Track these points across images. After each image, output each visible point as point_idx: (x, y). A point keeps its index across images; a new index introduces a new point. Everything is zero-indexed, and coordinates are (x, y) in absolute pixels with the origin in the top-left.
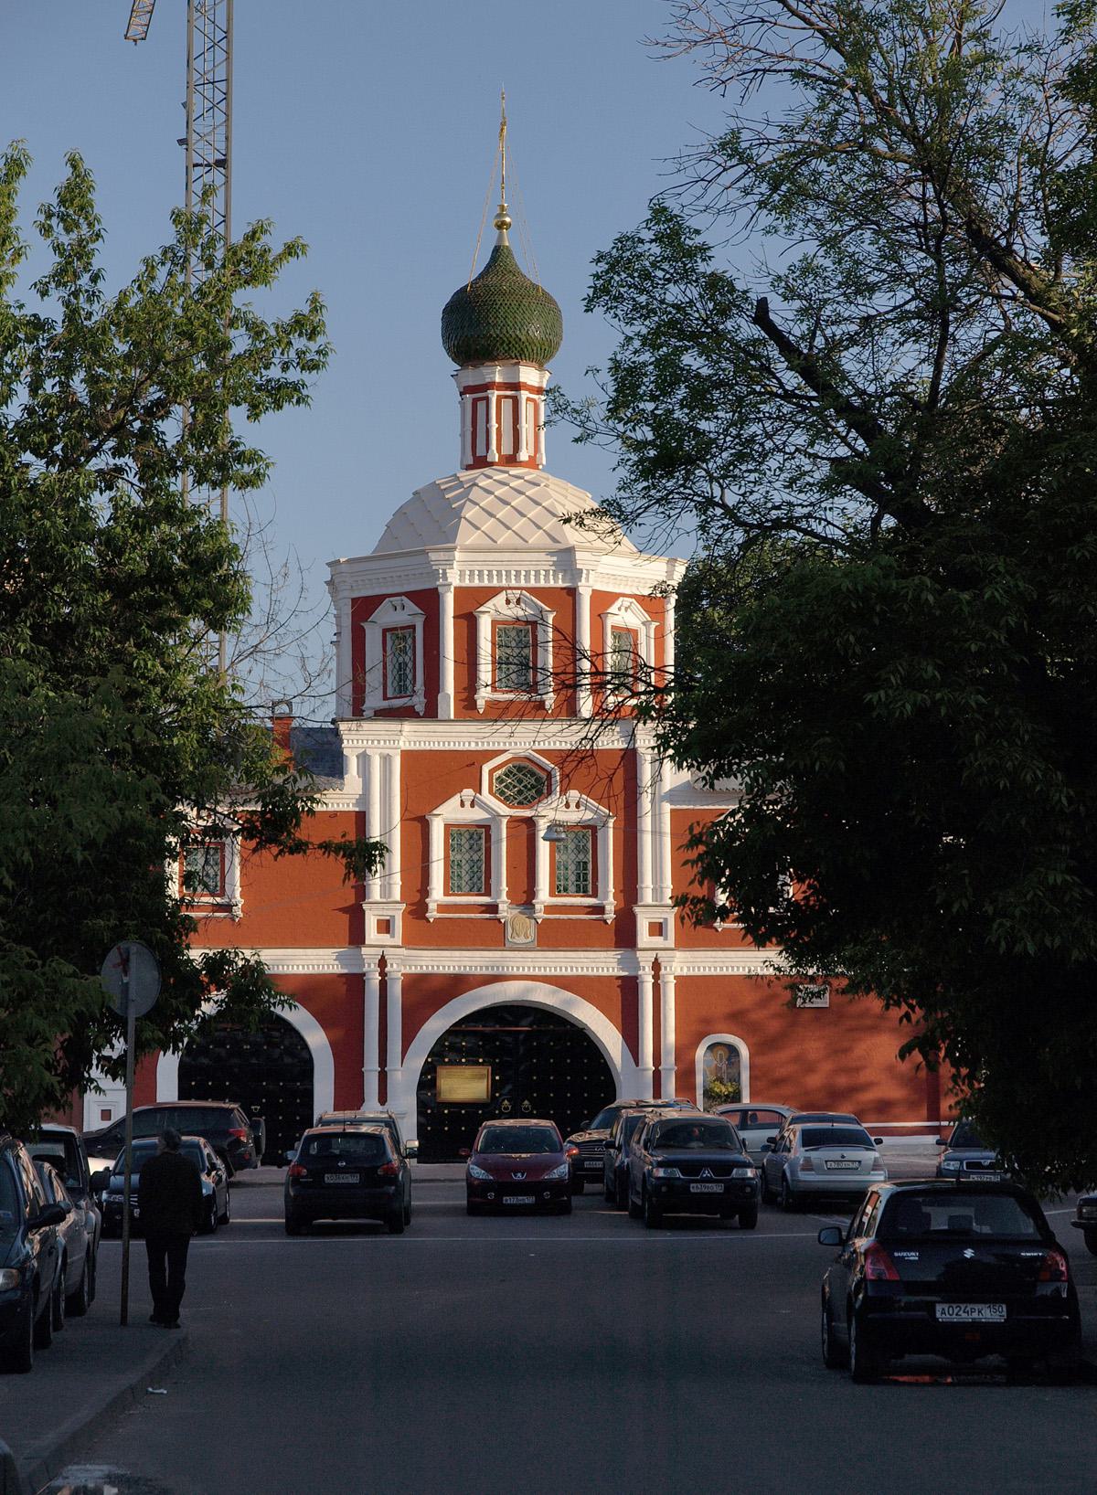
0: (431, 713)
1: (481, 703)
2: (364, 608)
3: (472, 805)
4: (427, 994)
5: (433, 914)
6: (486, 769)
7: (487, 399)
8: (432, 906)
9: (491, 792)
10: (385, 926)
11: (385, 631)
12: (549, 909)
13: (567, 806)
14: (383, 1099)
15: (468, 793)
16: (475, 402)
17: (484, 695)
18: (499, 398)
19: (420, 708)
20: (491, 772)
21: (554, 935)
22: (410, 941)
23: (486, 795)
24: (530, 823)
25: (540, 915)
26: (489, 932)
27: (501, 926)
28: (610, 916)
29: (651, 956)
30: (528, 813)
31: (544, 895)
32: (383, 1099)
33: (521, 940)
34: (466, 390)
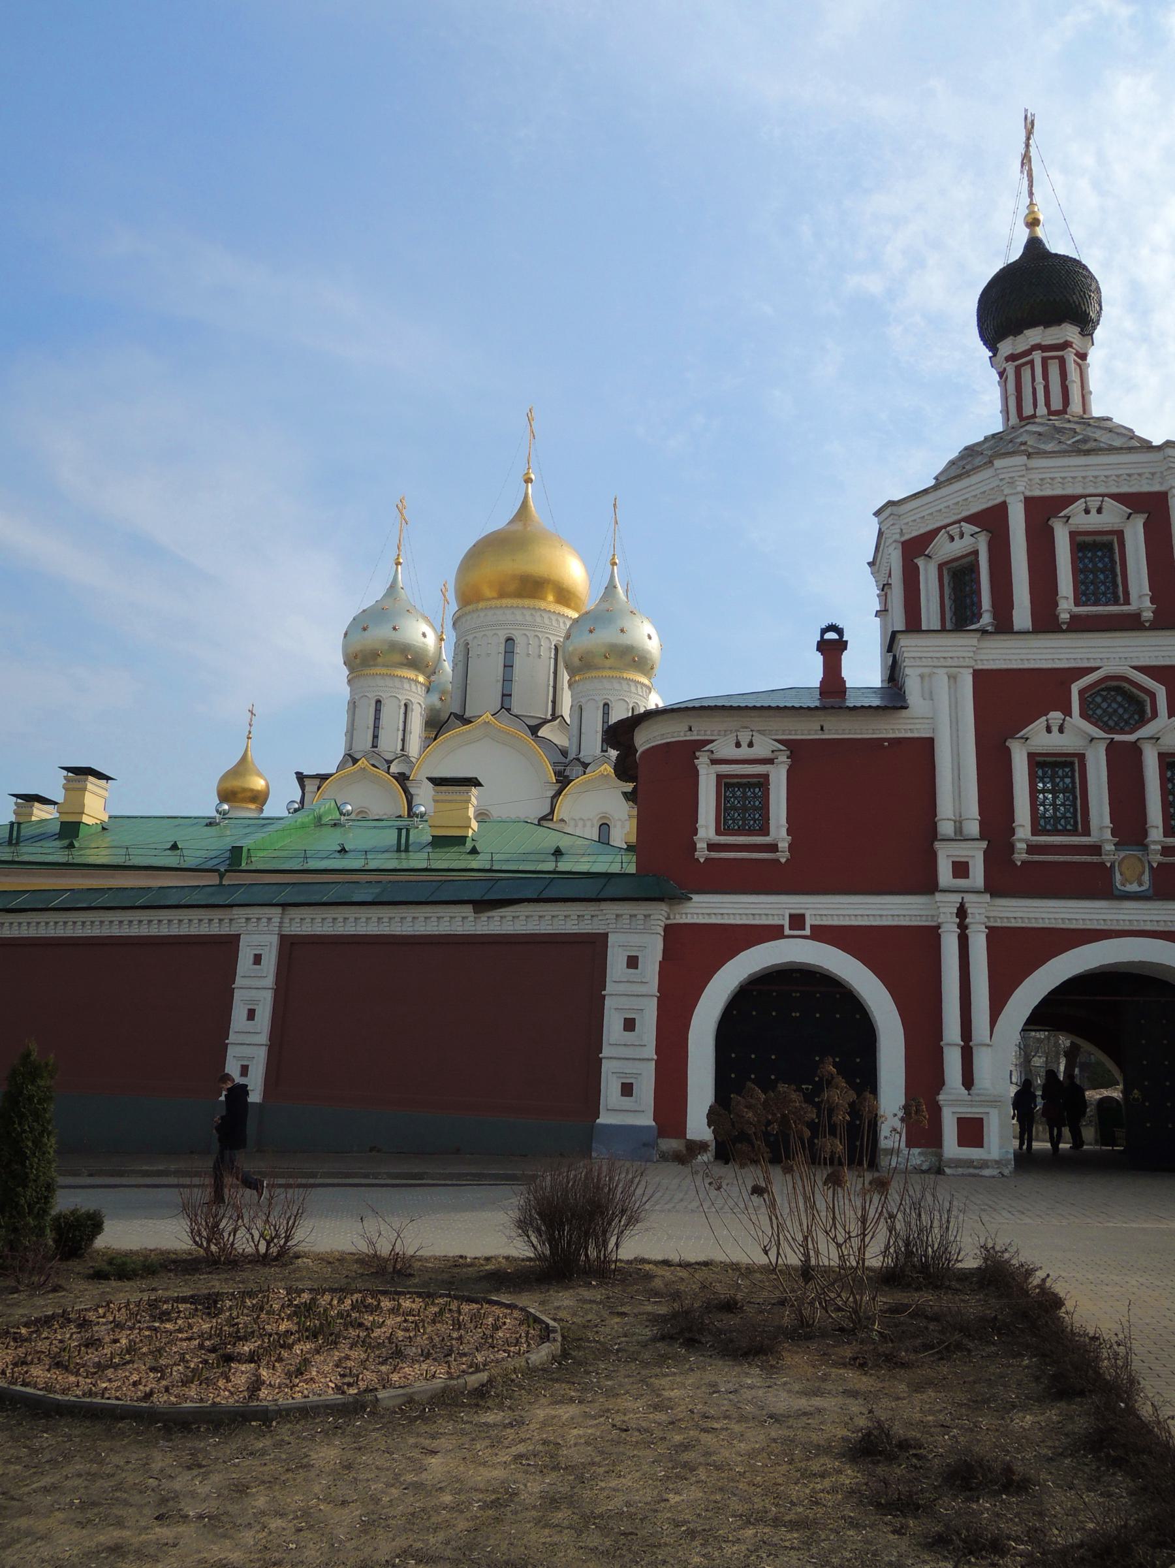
0: (1003, 625)
1: (1064, 616)
2: (915, 548)
3: (1061, 730)
5: (1020, 855)
6: (1075, 689)
7: (1032, 362)
8: (1021, 846)
9: (1081, 716)
10: (961, 869)
11: (940, 567)
14: (968, 1081)
15: (1056, 716)
16: (1018, 371)
17: (1066, 606)
18: (1045, 361)
20: (1081, 692)
22: (995, 888)
23: (1076, 719)
24: (1135, 750)
25: (1156, 859)
26: (1093, 882)
30: (1131, 738)
31: (1156, 833)
32: (968, 1081)
33: (1133, 888)
34: (1011, 358)
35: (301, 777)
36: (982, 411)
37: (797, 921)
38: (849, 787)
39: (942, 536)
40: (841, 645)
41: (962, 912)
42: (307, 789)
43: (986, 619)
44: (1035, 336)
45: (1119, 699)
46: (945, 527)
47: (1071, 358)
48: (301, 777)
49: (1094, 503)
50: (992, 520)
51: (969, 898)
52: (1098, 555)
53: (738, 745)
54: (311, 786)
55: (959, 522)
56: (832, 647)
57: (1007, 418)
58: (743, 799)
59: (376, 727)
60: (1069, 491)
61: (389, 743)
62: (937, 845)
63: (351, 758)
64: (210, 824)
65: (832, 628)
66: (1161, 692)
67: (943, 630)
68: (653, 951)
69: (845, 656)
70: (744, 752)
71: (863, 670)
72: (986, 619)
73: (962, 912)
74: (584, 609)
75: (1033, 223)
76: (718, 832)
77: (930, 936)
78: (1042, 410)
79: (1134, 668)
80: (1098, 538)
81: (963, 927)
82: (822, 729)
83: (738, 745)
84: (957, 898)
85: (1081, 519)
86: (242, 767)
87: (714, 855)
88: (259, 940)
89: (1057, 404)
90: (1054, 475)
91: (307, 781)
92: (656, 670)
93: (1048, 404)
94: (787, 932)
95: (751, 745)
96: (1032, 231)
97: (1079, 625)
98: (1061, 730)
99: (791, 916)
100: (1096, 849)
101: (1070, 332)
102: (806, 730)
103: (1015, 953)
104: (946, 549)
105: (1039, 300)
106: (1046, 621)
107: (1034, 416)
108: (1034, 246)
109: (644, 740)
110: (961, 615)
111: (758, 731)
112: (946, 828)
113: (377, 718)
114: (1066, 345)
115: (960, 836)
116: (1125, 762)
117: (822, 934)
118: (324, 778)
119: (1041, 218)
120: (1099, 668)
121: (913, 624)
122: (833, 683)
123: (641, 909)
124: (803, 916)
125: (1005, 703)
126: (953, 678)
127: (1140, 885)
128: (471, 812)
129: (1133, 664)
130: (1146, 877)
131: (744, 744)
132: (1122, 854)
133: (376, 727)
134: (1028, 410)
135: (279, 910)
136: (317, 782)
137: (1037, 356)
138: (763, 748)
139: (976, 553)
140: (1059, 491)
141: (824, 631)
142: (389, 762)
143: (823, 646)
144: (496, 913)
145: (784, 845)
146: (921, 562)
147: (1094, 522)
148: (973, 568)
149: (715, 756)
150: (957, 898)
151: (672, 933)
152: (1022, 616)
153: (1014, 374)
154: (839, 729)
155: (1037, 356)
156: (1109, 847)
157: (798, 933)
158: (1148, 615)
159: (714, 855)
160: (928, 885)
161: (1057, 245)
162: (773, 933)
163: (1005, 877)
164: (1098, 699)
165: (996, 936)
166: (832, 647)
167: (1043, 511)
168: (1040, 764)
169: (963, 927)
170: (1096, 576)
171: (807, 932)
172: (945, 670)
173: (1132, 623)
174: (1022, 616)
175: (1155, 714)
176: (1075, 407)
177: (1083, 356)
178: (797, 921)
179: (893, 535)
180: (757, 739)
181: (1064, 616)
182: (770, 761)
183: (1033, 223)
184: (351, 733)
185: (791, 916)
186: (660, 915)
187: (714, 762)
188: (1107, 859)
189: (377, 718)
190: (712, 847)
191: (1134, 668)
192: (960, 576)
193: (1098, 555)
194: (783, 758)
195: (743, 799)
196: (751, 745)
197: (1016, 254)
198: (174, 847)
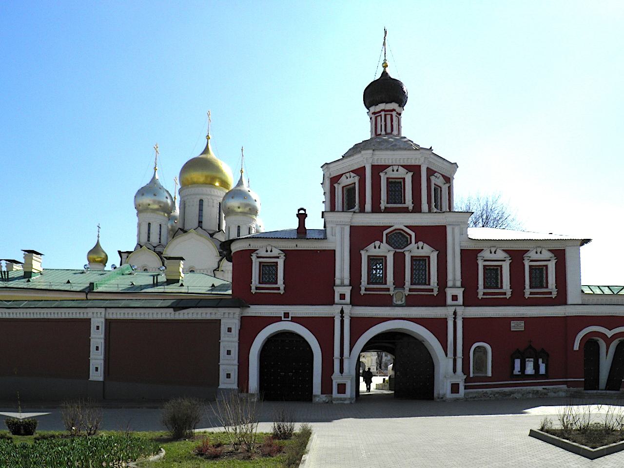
0: (362, 210)
1: (383, 207)
2: (335, 180)
4: (359, 325)
5: (363, 292)
6: (385, 233)
7: (381, 115)
8: (363, 289)
12: (410, 290)
13: (418, 248)
14: (342, 371)
15: (377, 243)
16: (376, 118)
17: (383, 205)
18: (385, 115)
19: (357, 211)
20: (387, 235)
21: (411, 301)
22: (353, 303)
23: (384, 246)
25: (407, 293)
26: (386, 301)
27: (391, 297)
28: (435, 293)
29: (452, 309)
32: (342, 371)
33: (399, 303)
34: (374, 113)
35: (120, 252)
36: (364, 132)
37: (286, 315)
38: (304, 266)
39: (344, 177)
40: (305, 215)
41: (342, 312)
42: (123, 257)
43: (357, 207)
44: (382, 106)
45: (400, 237)
46: (345, 174)
47: (394, 114)
48: (120, 252)
49: (395, 168)
50: (360, 172)
51: (344, 307)
52: (396, 186)
53: (267, 251)
54: (124, 256)
55: (349, 172)
56: (302, 216)
57: (372, 134)
58: (269, 270)
59: (149, 233)
60: (387, 163)
61: (154, 239)
62: (335, 288)
63: (140, 245)
64: (82, 273)
65: (302, 209)
66: (413, 234)
67: (343, 211)
68: (235, 324)
69: (306, 220)
70: (269, 254)
71: (314, 223)
72: (357, 207)
73: (342, 312)
74: (231, 189)
75: (385, 66)
76: (260, 283)
77: (332, 319)
78: (383, 133)
79: (406, 226)
80: (397, 180)
81: (342, 317)
82: (297, 246)
83: (267, 251)
84: (340, 307)
85: (390, 173)
86: (97, 249)
87: (258, 291)
88: (98, 319)
89: (389, 130)
90: (383, 157)
91: (122, 254)
92: (259, 213)
93: (385, 130)
94: (283, 319)
95: (271, 251)
96: (385, 69)
97: (388, 211)
98: (379, 248)
99: (285, 313)
100: (388, 290)
101: (393, 106)
102: (291, 246)
103: (359, 325)
104: (345, 181)
105: (385, 94)
106: (376, 209)
107: (380, 135)
108: (385, 74)
109: (235, 248)
110: (349, 205)
111: (274, 247)
112: (338, 282)
113: (149, 230)
114: (394, 110)
115: (342, 285)
116: (399, 259)
117: (295, 320)
118: (129, 253)
119: (388, 64)
120: (392, 226)
121: (333, 208)
122: (302, 230)
123: (232, 310)
124: (288, 313)
125: (361, 237)
126: (342, 230)
127: (402, 301)
128: (181, 270)
129: (405, 225)
130: (404, 299)
131: (269, 251)
132: (397, 291)
133: (149, 233)
134: (379, 132)
135: (104, 309)
136: (126, 254)
137: (383, 113)
138: (276, 252)
139: (355, 183)
140: (383, 163)
141: (299, 210)
142: (154, 247)
143: (298, 215)
144: (182, 312)
145: (282, 288)
146: (336, 185)
147: (395, 175)
148: (354, 188)
149: (259, 255)
150: (340, 307)
151: (243, 319)
152: (368, 207)
153: (375, 117)
154: (303, 245)
155: (383, 113)
156: (392, 288)
157: (287, 319)
158: (411, 208)
159: (258, 291)
160: (332, 303)
161: (393, 74)
162: (278, 319)
163: (357, 300)
164: (393, 237)
165: (352, 319)
166: (302, 216)
167: (377, 169)
168: (372, 260)
169: (342, 317)
170: (395, 193)
171: (290, 319)
172: (340, 226)
173: (405, 210)
174: (368, 207)
175: (411, 243)
176: (395, 132)
177: (400, 114)
178: (286, 315)
179: (327, 175)
180: (274, 249)
181: (383, 207)
182: (278, 257)
183: (385, 66)
184: (139, 235)
185: (285, 313)
186: (237, 311)
187: (258, 257)
188: (391, 293)
189: (149, 230)
190: (257, 288)
191: (406, 226)
192: (349, 191)
193: (396, 186)
194: (282, 256)
195: (269, 270)
196: (271, 251)
197: (378, 76)
198: (68, 282)
